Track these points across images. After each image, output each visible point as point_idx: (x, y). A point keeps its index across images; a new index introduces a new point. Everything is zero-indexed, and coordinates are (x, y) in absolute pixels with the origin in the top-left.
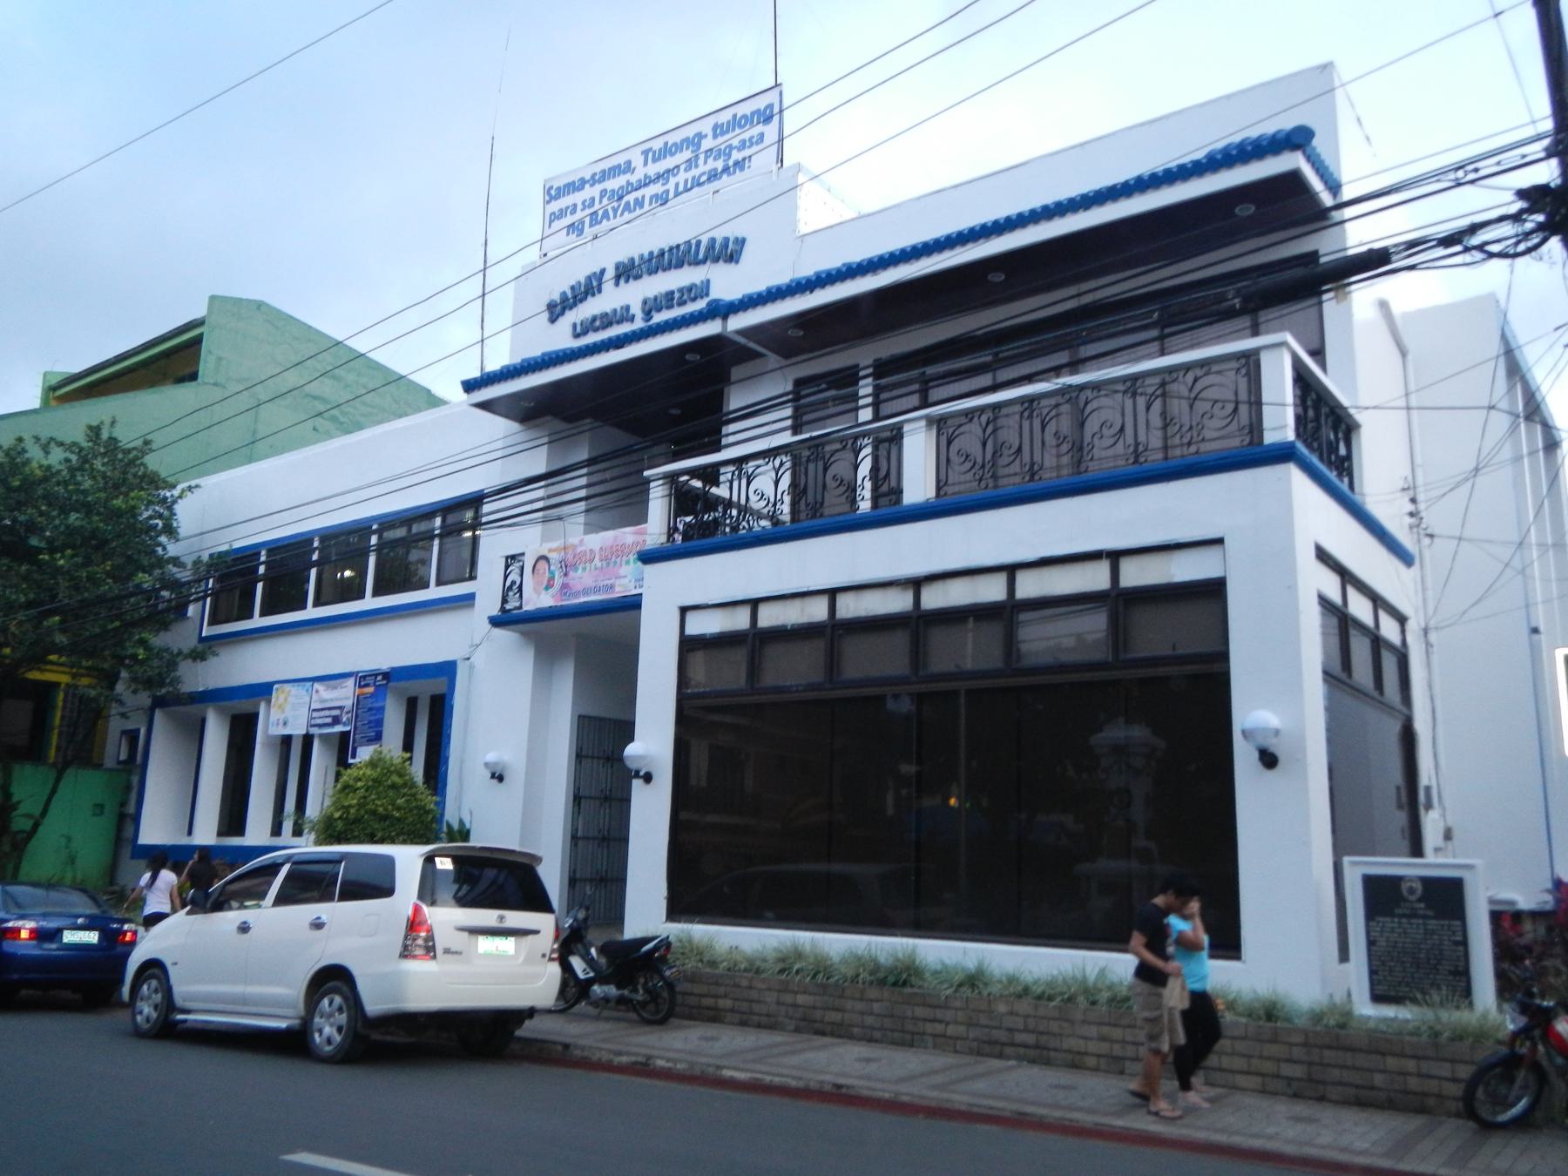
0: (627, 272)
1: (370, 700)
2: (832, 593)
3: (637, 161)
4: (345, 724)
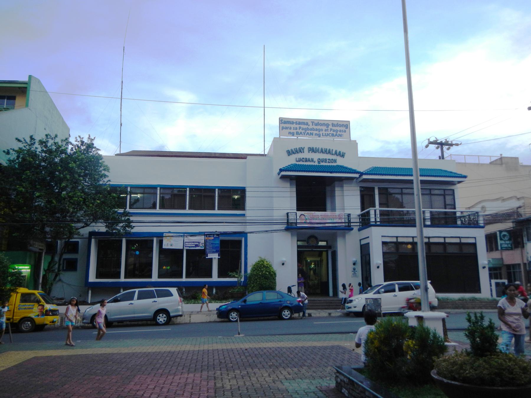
0: (312, 150)
1: (212, 241)
3: (310, 124)
4: (201, 247)
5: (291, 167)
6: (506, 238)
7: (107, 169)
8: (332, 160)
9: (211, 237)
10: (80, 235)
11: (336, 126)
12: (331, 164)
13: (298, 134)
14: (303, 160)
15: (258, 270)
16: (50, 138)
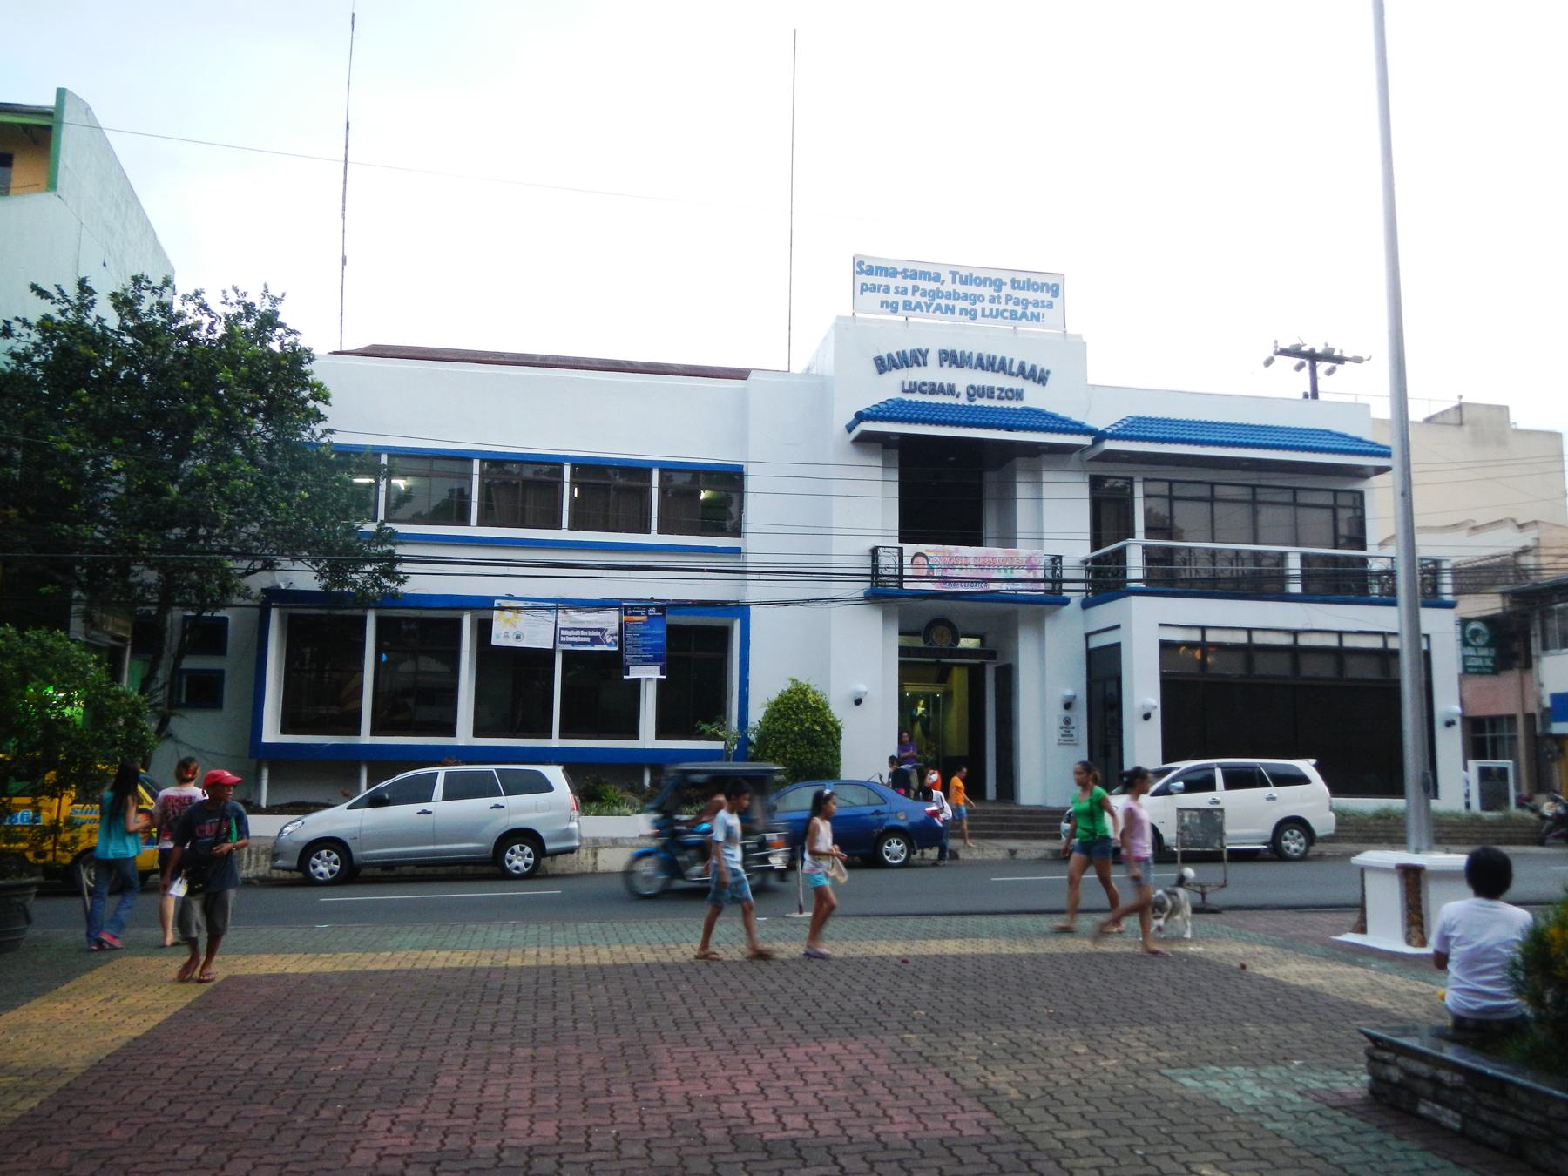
0: (951, 359)
1: (643, 627)
2: (1250, 631)
3: (947, 277)
4: (609, 645)
5: (888, 409)
6: (1480, 641)
7: (321, 395)
8: (1011, 390)
9: (639, 614)
10: (250, 598)
11: (1023, 289)
12: (1006, 404)
13: (910, 309)
14: (924, 388)
15: (789, 719)
16: (147, 289)
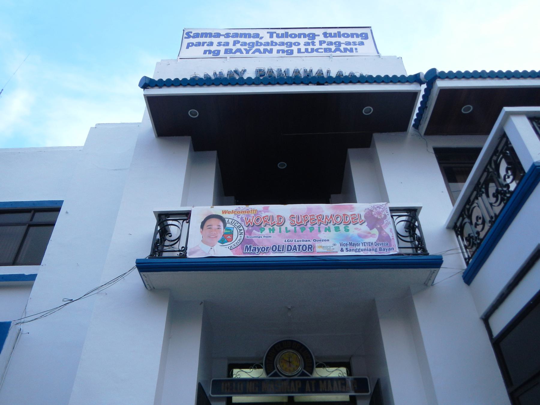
3: (264, 34)
